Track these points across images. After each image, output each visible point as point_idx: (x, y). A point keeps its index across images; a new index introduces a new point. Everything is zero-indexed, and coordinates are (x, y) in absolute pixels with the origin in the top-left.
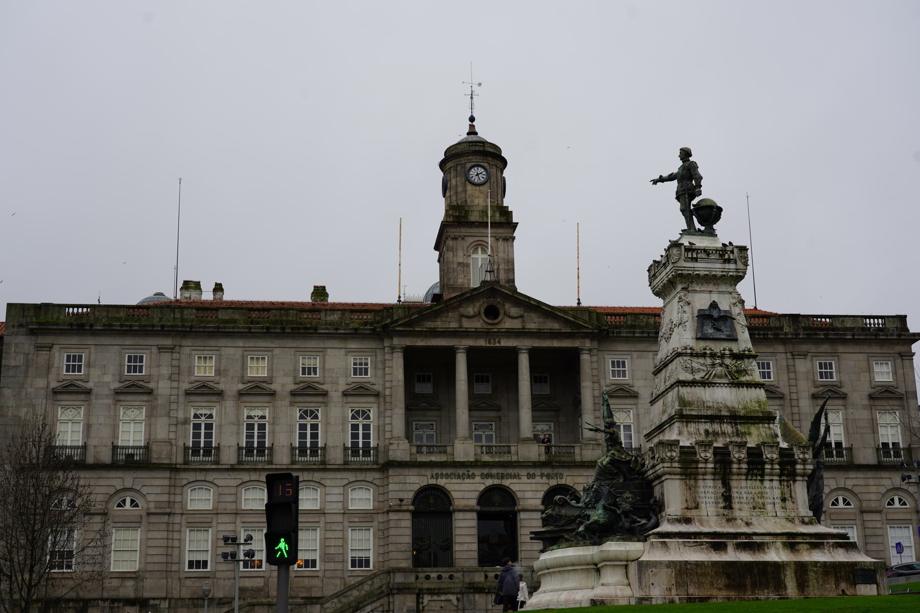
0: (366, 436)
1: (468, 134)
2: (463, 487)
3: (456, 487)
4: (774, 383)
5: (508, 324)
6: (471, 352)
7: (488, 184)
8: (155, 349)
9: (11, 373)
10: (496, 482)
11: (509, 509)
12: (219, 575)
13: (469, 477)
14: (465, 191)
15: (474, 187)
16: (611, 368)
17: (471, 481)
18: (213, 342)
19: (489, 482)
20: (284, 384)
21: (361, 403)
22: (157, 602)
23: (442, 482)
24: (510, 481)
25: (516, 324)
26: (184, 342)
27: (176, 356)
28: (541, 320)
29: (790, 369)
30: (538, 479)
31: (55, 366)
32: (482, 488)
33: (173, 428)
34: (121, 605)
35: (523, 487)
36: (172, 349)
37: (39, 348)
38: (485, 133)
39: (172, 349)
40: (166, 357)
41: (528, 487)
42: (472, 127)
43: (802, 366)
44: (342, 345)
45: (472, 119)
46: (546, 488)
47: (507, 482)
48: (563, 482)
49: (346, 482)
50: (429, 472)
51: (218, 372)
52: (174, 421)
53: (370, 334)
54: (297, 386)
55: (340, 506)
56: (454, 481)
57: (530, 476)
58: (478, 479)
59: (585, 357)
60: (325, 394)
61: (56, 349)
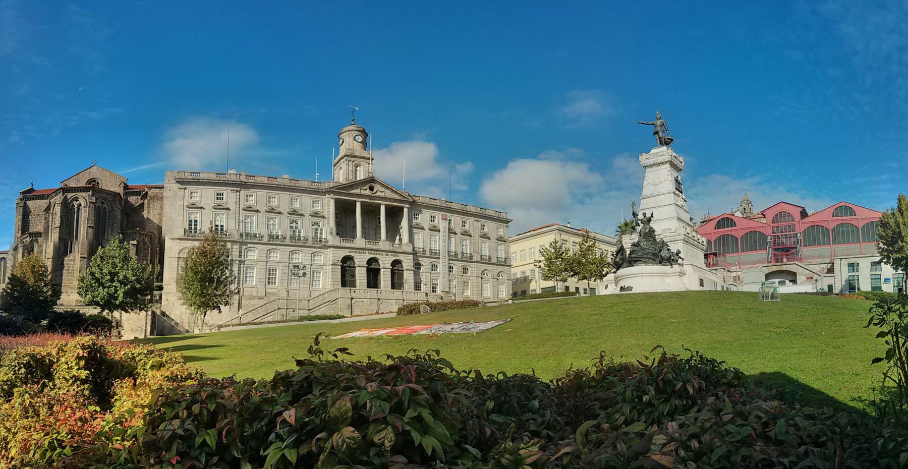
0: (321, 234)
2: (361, 257)
3: (359, 257)
5: (378, 194)
8: (229, 191)
10: (373, 256)
11: (378, 267)
17: (365, 255)
20: (284, 209)
23: (352, 254)
27: (238, 194)
33: (237, 224)
35: (384, 259)
41: (386, 259)
47: (377, 256)
48: (398, 258)
50: (348, 250)
54: (289, 210)
57: (387, 255)
59: (406, 210)
60: (302, 215)
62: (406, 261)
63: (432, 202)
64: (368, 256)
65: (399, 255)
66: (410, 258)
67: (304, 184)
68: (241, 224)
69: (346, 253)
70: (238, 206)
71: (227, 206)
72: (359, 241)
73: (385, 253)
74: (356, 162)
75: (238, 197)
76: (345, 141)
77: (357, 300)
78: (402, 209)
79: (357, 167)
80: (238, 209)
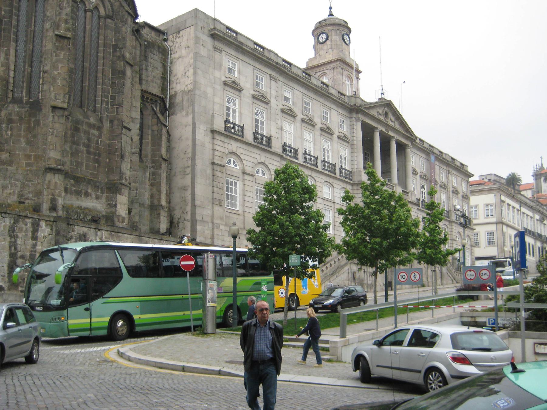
1: (329, 15)
14: (342, 45)
15: (346, 45)
18: (290, 83)
26: (281, 78)
29: (447, 178)
31: (224, 65)
36: (276, 80)
39: (275, 80)
40: (273, 83)
42: (331, 12)
43: (450, 176)
44: (336, 109)
45: (331, 8)
51: (293, 102)
53: (348, 108)
76: (329, 38)
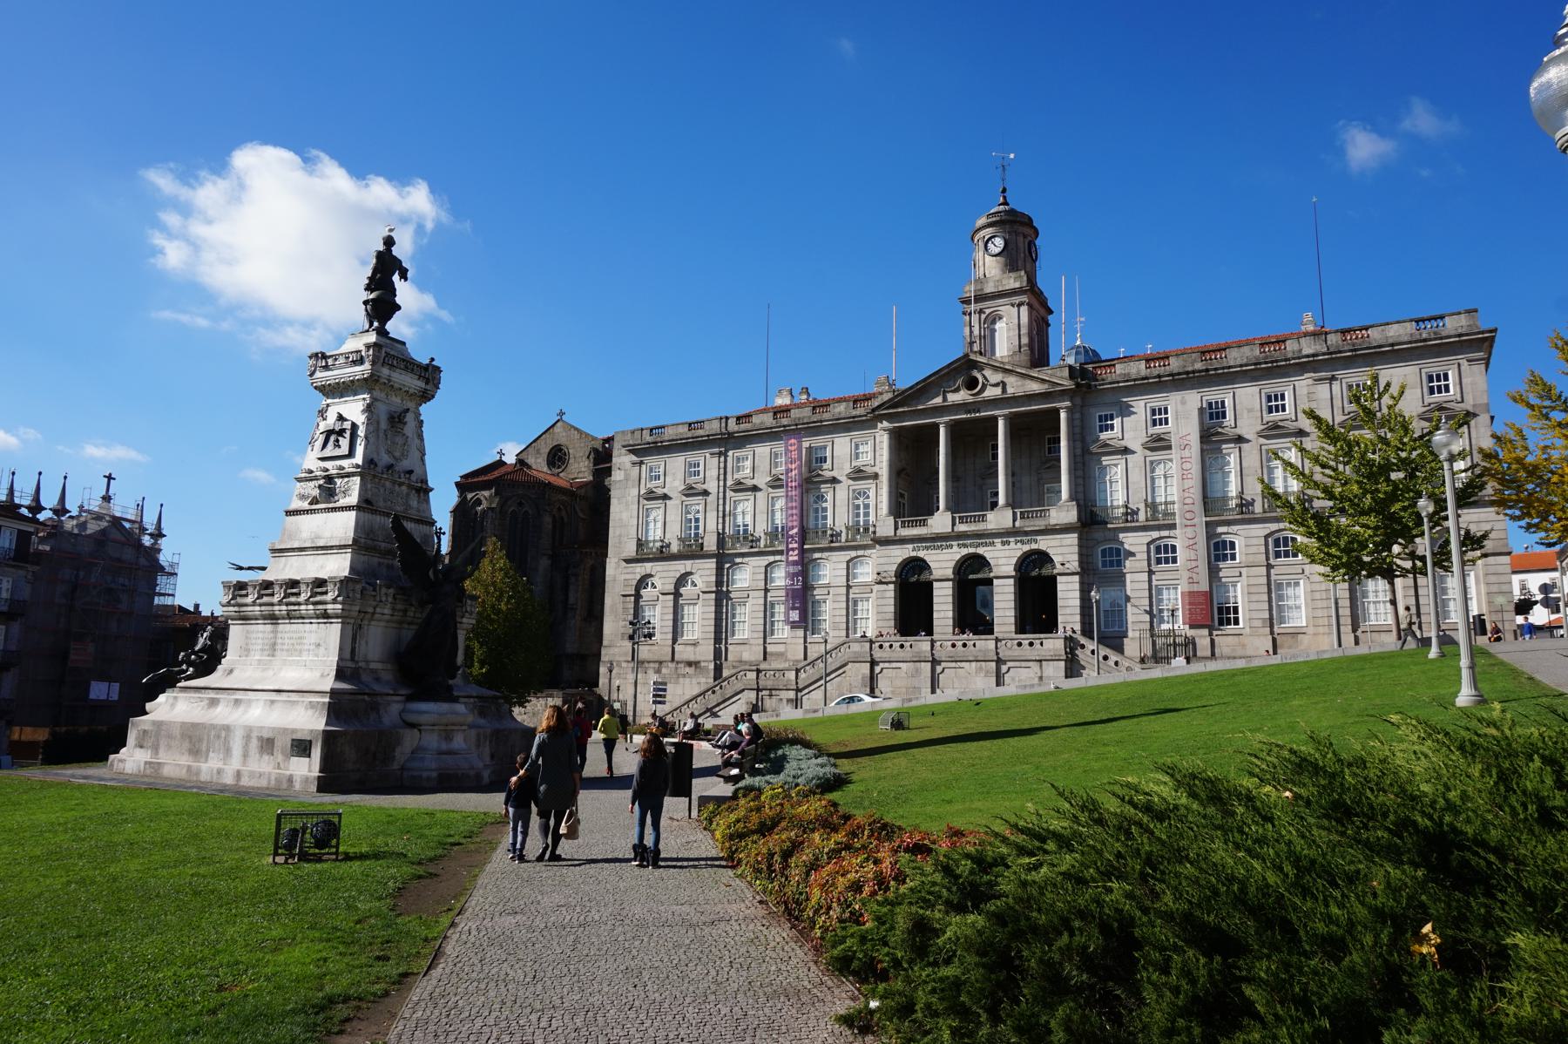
0: (867, 514)
2: (941, 557)
3: (935, 558)
4: (1288, 417)
6: (954, 428)
7: (1005, 253)
8: (708, 455)
9: (617, 485)
10: (972, 550)
12: (752, 641)
13: (947, 547)
16: (1098, 424)
17: (950, 551)
19: (965, 551)
21: (861, 485)
22: (706, 664)
23: (921, 554)
24: (985, 548)
25: (997, 391)
28: (1020, 383)
30: (1012, 545)
32: (958, 557)
33: (721, 520)
34: (682, 665)
35: (997, 554)
37: (634, 464)
38: (1015, 204)
46: (1019, 554)
47: (980, 551)
48: (1034, 546)
49: (848, 558)
52: (721, 514)
55: (844, 579)
56: (933, 552)
57: (1003, 543)
58: (955, 548)
59: (1063, 415)
61: (644, 467)
62: (1060, 550)
63: (1158, 369)
64: (956, 553)
65: (1039, 538)
66: (1068, 542)
67: (837, 410)
68: (727, 519)
69: (906, 552)
70: (722, 483)
71: (705, 487)
72: (940, 522)
73: (1000, 540)
74: (988, 311)
75: (722, 465)
77: (887, 665)
78: (1056, 412)
79: (994, 322)
80: (721, 489)
